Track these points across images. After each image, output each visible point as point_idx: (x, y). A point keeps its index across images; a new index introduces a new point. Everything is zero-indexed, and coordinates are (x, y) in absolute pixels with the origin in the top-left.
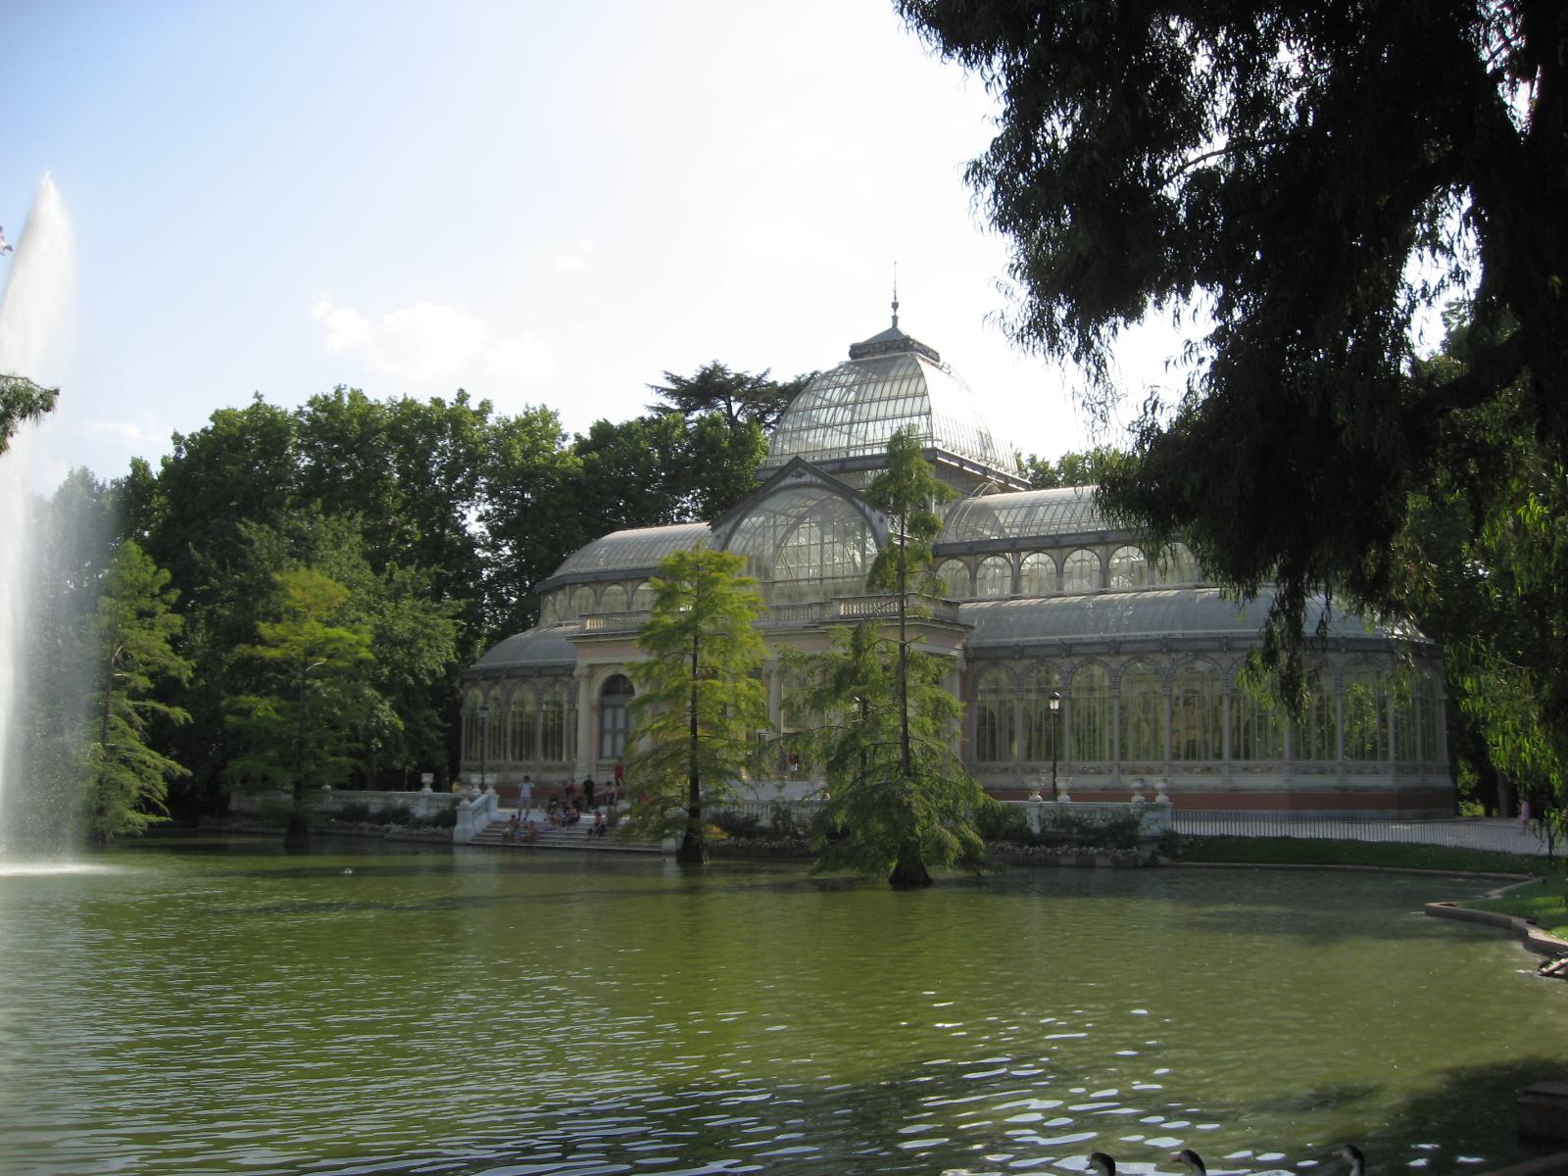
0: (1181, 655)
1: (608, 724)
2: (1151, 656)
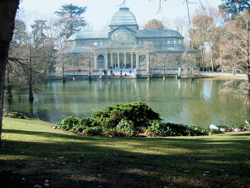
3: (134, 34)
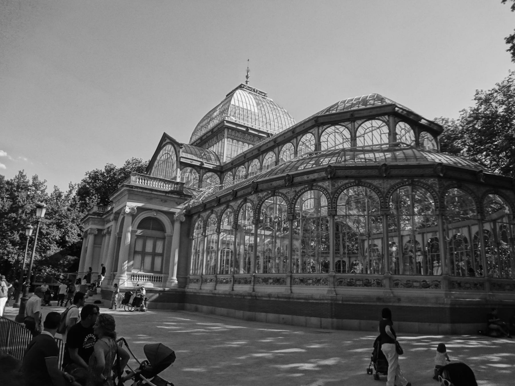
0: (265, 193)
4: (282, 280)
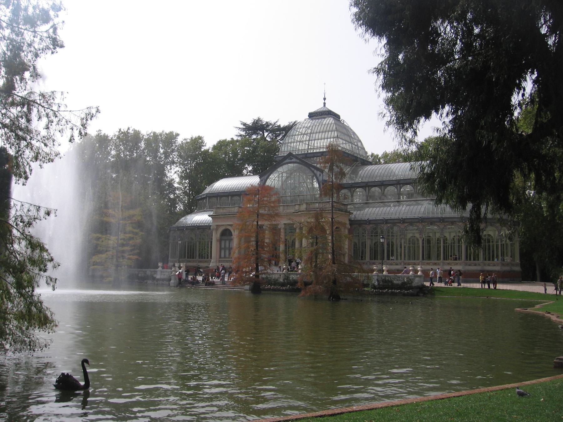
0: (426, 223)
1: (223, 246)
2: (415, 224)
3: (318, 175)
4: (437, 263)
